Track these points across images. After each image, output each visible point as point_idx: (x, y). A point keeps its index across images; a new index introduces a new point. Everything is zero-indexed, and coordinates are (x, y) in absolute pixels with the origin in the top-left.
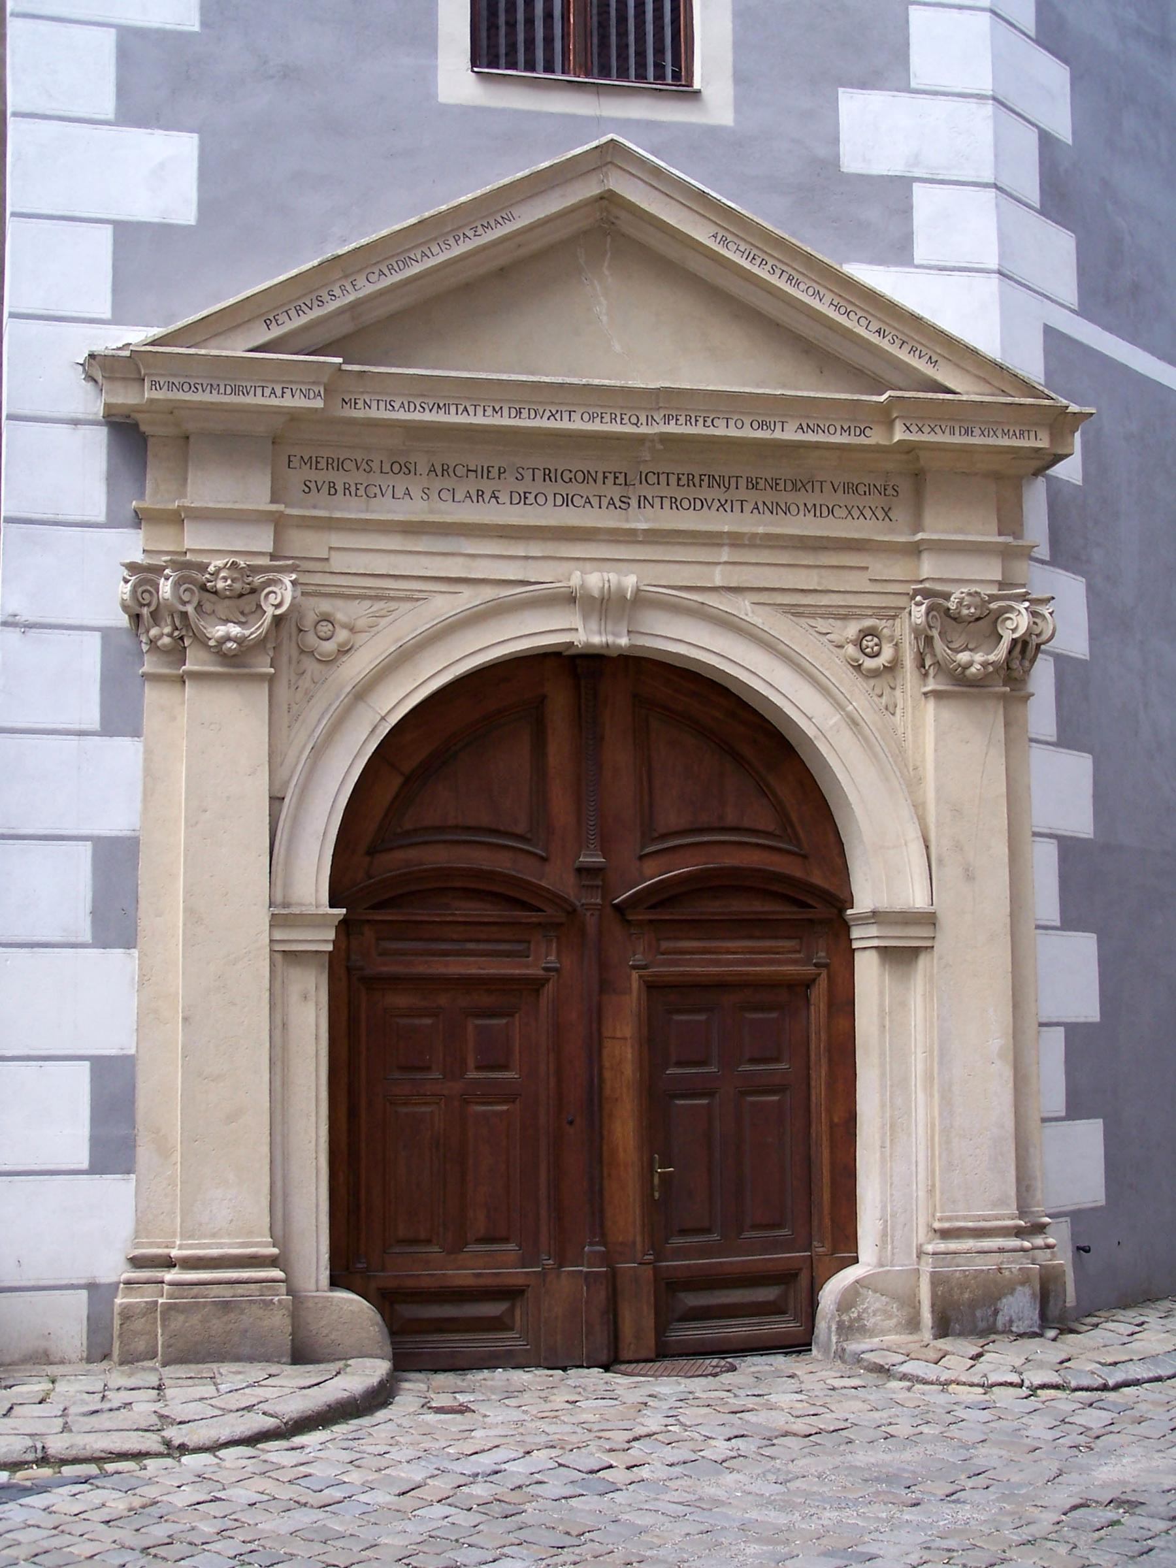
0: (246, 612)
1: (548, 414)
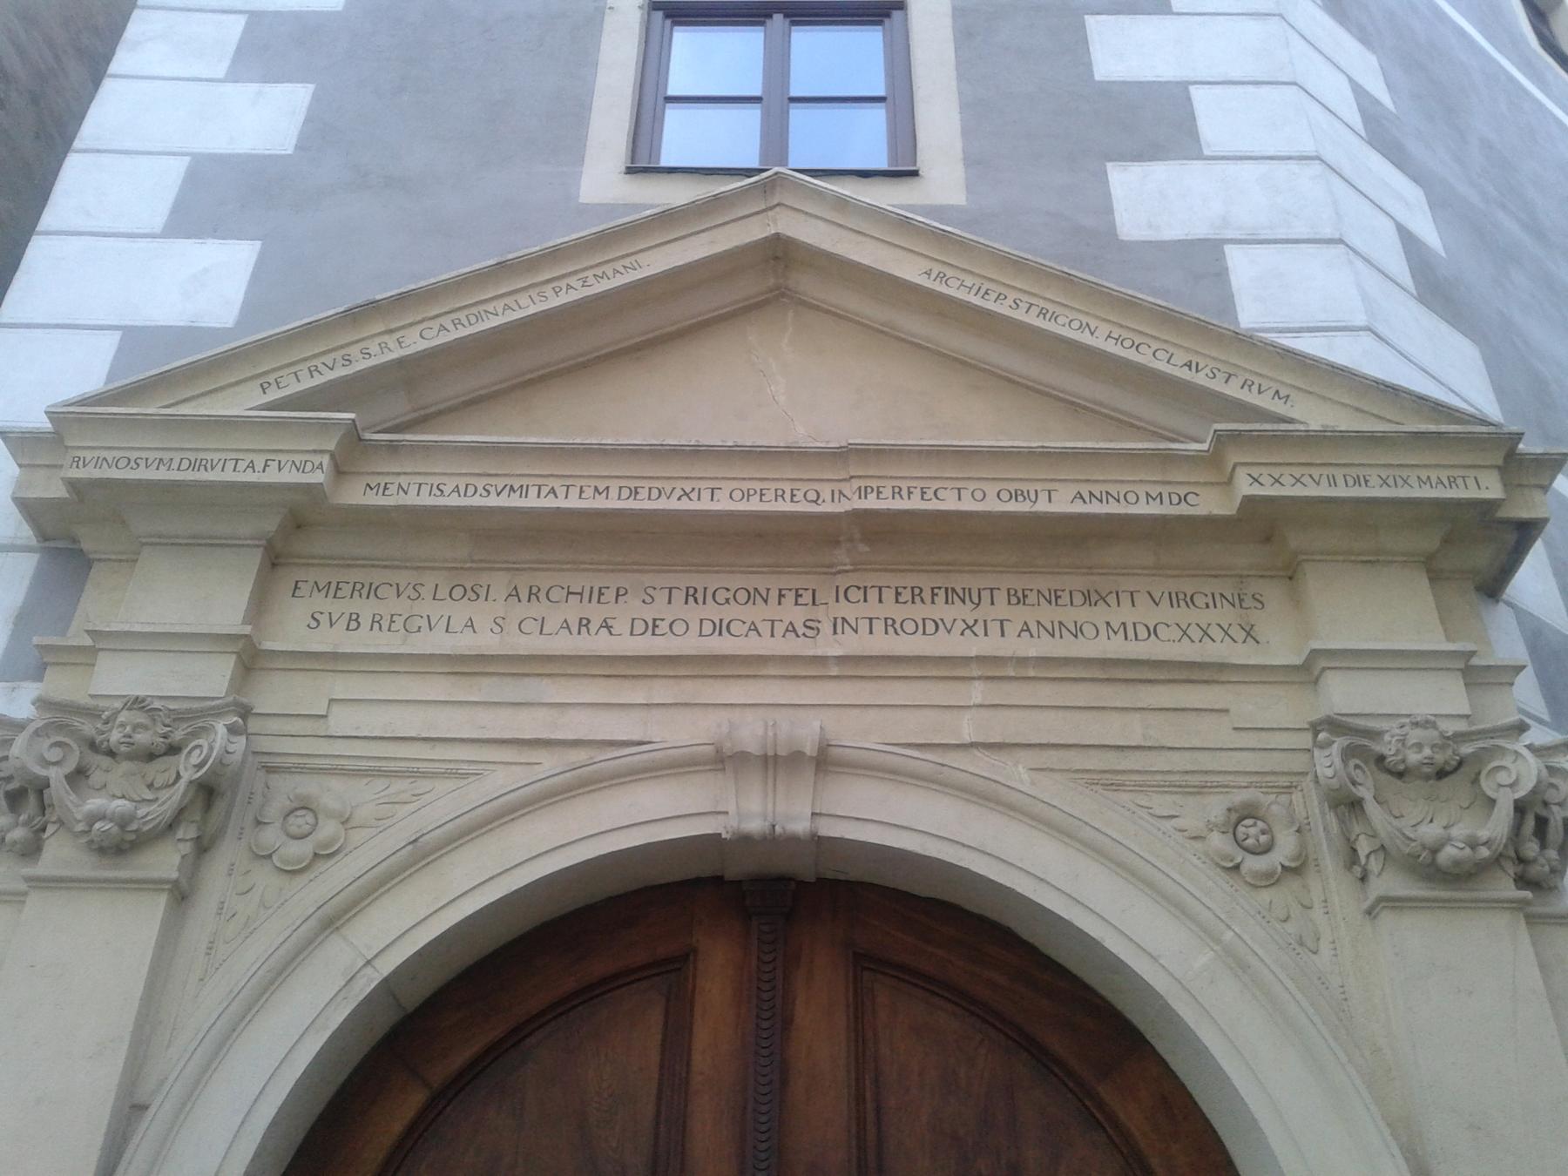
0: (156, 785)
1: (678, 492)
